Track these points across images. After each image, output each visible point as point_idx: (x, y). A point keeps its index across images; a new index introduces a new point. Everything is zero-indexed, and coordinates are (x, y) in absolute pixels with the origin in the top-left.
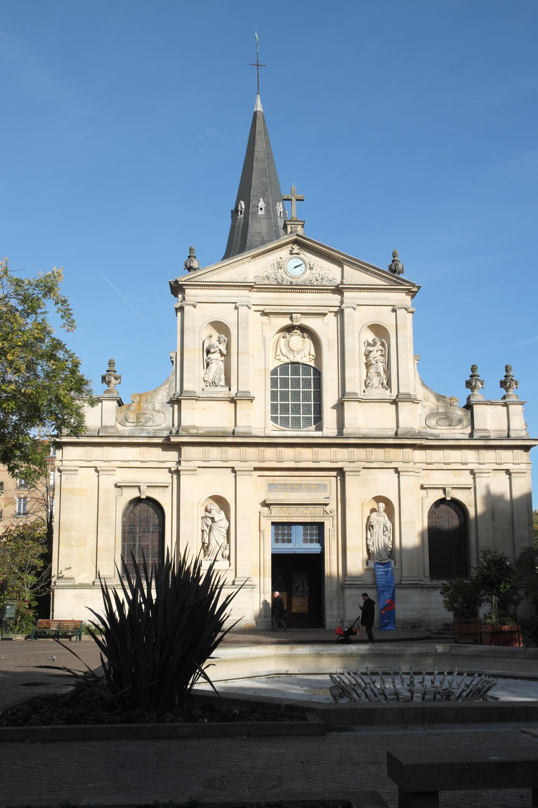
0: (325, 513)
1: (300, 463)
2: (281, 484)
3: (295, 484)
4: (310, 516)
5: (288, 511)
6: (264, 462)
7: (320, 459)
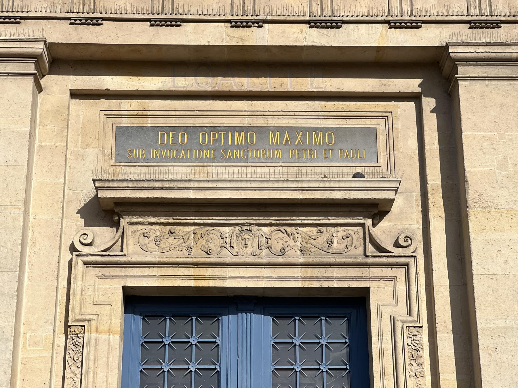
0: (370, 248)
1: (254, 29)
2: (174, 129)
3: (233, 129)
4: (301, 261)
5: (203, 242)
6: (96, 22)
7: (342, 13)
